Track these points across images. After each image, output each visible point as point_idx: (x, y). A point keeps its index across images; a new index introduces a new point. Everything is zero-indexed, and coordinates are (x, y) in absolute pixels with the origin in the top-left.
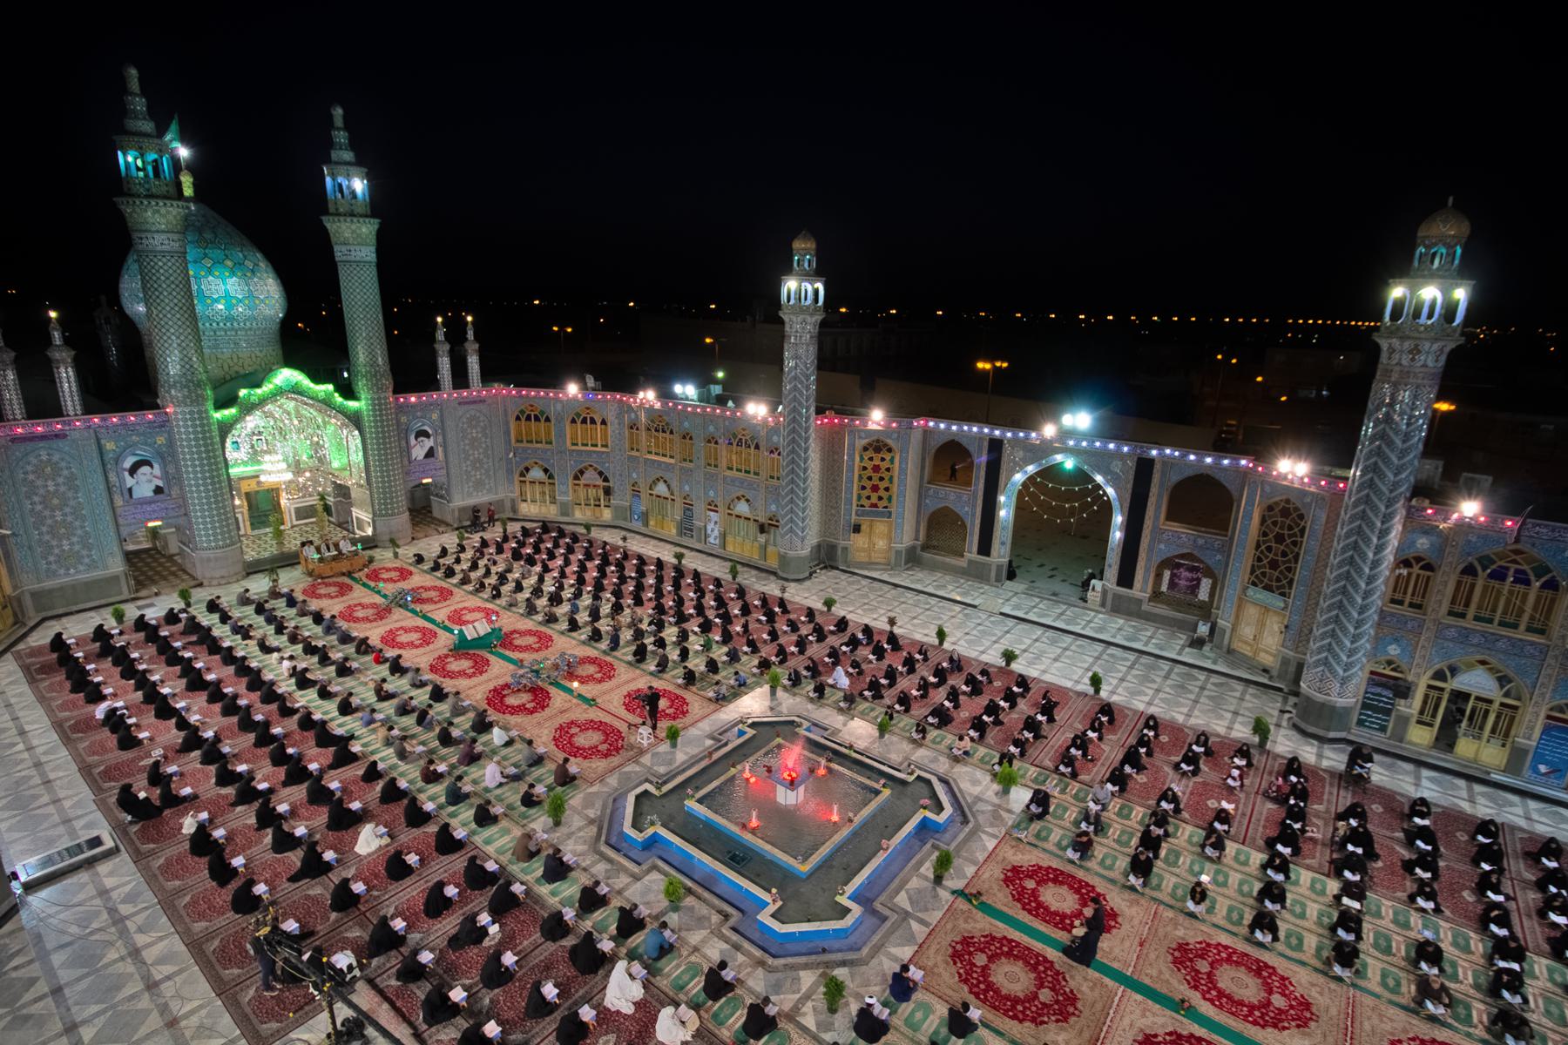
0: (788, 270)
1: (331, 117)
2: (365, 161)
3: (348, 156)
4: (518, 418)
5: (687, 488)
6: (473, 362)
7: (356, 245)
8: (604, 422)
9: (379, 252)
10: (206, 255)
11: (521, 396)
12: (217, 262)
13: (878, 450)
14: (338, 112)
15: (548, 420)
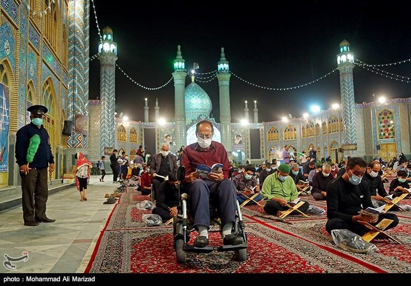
0: (339, 53)
1: (221, 51)
2: (229, 59)
3: (224, 59)
4: (269, 132)
5: (318, 145)
6: (256, 115)
7: (225, 82)
8: (295, 130)
9: (230, 83)
10: (193, 93)
11: (270, 125)
12: (197, 95)
13: (385, 114)
14: (223, 49)
15: (278, 131)
